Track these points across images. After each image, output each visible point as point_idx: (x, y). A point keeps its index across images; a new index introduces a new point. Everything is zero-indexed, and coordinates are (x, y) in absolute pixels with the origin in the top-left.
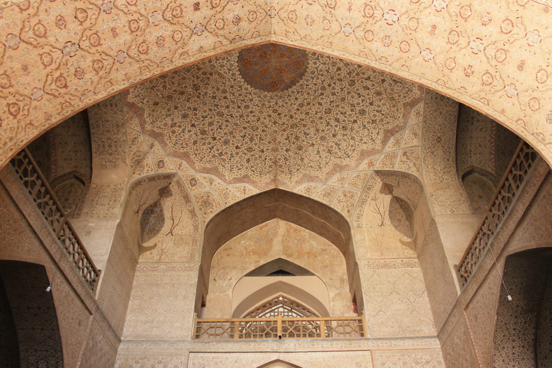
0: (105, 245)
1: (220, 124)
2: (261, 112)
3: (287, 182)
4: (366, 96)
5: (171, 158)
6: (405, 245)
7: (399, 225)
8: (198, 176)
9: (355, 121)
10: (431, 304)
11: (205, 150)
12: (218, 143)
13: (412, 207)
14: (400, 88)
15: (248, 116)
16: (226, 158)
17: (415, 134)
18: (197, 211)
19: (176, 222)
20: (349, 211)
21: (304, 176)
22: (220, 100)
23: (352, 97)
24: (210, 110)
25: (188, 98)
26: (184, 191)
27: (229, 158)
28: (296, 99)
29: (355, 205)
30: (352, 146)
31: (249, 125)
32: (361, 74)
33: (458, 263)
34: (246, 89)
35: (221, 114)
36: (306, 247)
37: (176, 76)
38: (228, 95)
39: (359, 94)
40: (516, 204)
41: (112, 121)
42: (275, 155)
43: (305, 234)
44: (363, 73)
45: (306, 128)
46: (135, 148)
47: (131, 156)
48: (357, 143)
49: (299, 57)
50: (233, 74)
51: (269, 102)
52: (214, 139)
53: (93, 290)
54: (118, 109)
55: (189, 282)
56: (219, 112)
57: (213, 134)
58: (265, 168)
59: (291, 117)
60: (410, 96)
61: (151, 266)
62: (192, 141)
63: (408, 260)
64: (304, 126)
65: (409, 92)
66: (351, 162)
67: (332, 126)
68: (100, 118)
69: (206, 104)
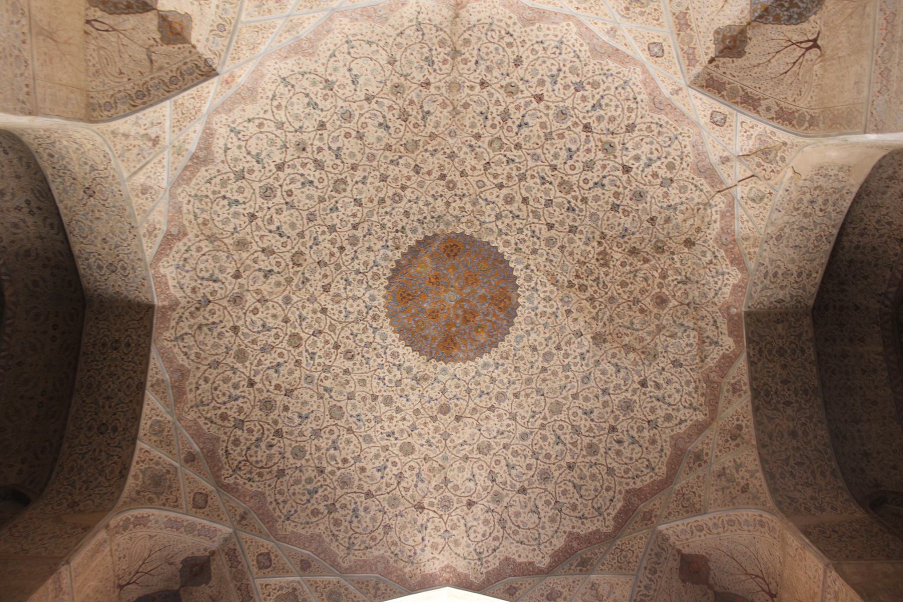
1: (570, 162)
2: (481, 184)
4: (267, 233)
5: (693, 117)
8: (643, 56)
9: (280, 168)
11: (613, 104)
12: (581, 116)
14: (202, 266)
15: (509, 177)
17: (145, 190)
21: (387, 19)
22: (562, 223)
23: (293, 226)
24: (584, 200)
25: (624, 236)
26: (682, 42)
27: (562, 75)
30: (279, 107)
32: (283, 282)
37: (636, 293)
38: (545, 233)
39: (281, 235)
41: (787, 246)
42: (455, 74)
44: (278, 284)
45: (385, 141)
46: (762, 186)
48: (269, 116)
49: (403, 311)
50: (529, 279)
52: (587, 128)
56: (568, 193)
57: (587, 141)
58: (479, 39)
59: (417, 170)
60: (177, 256)
64: (389, 147)
65: (181, 263)
66: (274, 68)
67: (330, 148)
68: (808, 252)
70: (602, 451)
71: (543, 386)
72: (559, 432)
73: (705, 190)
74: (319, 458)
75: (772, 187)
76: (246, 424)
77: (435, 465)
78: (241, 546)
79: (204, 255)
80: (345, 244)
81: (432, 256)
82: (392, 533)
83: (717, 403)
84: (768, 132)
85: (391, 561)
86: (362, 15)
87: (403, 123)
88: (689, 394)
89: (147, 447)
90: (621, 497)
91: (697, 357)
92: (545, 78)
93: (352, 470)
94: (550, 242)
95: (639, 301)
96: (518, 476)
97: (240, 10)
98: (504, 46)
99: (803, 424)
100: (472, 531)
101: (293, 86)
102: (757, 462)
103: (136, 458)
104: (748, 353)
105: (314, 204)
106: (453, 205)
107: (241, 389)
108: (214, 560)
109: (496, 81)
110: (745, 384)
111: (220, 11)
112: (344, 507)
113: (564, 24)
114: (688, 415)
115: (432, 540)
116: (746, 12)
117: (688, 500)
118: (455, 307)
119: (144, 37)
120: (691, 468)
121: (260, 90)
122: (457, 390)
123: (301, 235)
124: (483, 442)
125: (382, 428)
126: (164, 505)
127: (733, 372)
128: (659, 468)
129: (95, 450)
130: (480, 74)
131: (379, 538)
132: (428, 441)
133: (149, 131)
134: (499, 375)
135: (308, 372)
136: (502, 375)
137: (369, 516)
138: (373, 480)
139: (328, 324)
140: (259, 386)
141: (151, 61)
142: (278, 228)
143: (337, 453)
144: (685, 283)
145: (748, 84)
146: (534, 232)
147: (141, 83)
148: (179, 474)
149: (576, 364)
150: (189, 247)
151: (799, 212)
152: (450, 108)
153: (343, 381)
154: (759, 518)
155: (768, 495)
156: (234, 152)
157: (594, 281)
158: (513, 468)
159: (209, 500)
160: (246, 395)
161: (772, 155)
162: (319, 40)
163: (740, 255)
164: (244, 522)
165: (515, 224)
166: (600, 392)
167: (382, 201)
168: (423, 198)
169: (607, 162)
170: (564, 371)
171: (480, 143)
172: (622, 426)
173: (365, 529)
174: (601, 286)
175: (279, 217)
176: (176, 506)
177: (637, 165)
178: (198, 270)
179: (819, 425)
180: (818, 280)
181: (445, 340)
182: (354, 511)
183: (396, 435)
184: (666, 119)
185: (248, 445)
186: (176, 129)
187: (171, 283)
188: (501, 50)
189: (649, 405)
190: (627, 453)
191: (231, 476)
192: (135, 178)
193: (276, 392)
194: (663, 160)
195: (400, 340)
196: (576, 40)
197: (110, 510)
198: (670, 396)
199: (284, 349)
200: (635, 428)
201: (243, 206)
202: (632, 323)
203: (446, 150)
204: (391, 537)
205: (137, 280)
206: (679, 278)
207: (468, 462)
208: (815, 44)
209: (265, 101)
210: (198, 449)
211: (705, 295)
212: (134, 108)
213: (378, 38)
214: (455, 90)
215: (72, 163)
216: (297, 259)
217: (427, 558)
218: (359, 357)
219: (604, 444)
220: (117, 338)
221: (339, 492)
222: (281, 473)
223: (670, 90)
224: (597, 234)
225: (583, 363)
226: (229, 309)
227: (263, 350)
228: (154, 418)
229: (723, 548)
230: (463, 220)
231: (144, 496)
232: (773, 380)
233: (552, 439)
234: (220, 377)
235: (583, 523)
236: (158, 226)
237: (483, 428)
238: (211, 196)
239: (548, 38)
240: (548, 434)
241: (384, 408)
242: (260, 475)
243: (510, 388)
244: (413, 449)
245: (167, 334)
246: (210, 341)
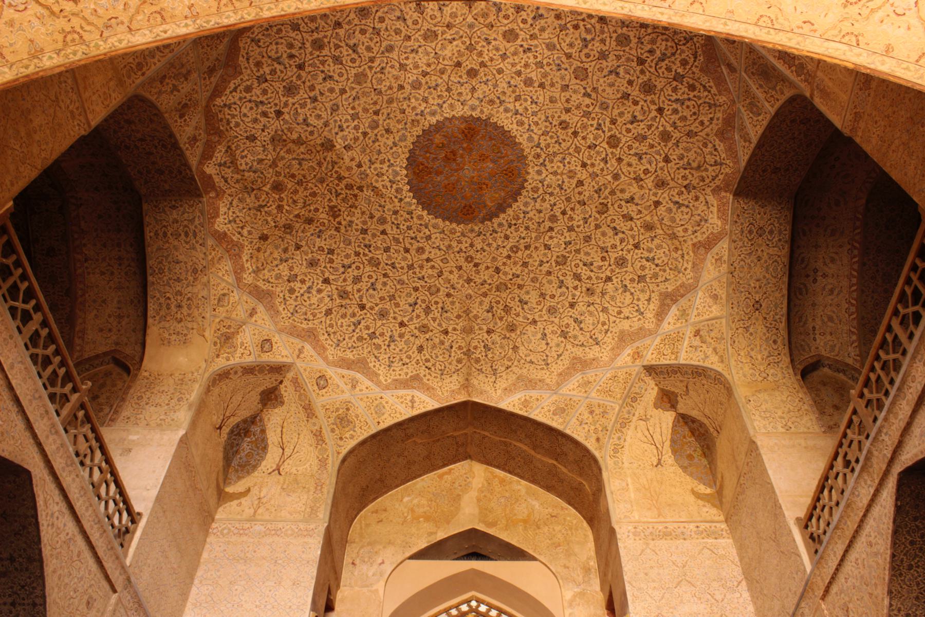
0: (154, 472)
1: (373, 280)
3: (488, 389)
4: (627, 232)
5: (284, 336)
6: (702, 499)
7: (690, 465)
8: (331, 372)
10: (755, 603)
11: (345, 328)
12: (368, 315)
13: (712, 430)
14: (686, 217)
15: (421, 267)
17: (715, 297)
18: (326, 433)
19: (288, 452)
20: (598, 440)
21: (518, 378)
22: (374, 236)
24: (357, 254)
25: (320, 231)
26: (306, 396)
27: (387, 343)
28: (507, 237)
29: (609, 429)
30: (604, 324)
31: (424, 284)
33: (802, 513)
34: (420, 217)
36: (521, 511)
37: (301, 189)
38: (388, 227)
39: (615, 228)
40: (910, 366)
41: (186, 263)
43: (519, 487)
44: (622, 191)
48: (612, 319)
49: (512, 161)
51: (460, 242)
52: (363, 307)
53: (122, 545)
54: (197, 242)
55: (304, 556)
56: (372, 258)
57: (361, 298)
59: (497, 270)
60: (704, 230)
61: (237, 525)
62: (324, 310)
63: (708, 525)
64: (520, 287)
65: (703, 223)
66: (602, 353)
67: (567, 288)
68: (167, 257)
69: (350, 244)
70: (308, 45)
72: (354, 56)
81: (485, 206)
88: (233, 116)
89: (767, 104)
92: (398, 339)
95: (298, 183)
97: (618, 414)
99: (123, 128)
101: (591, 337)
103: (778, 105)
104: (191, 170)
106: (467, 245)
107: (671, 108)
110: (187, 149)
113: (389, 381)
114: (230, 97)
116: (266, 419)
118: (464, 164)
120: (217, 59)
123: (597, 227)
124: (432, 42)
125: (535, 57)
127: (199, 151)
132: (489, 43)
134: (420, 105)
136: (417, 106)
140: (653, 107)
143: (584, 35)
144: (261, 206)
149: (347, 121)
152: (471, 315)
154: (144, 69)
156: (643, 297)
158: (399, 18)
160: (666, 102)
162: (568, 368)
163: (220, 243)
166: (319, 98)
167: (527, 247)
168: (493, 249)
172: (292, 72)
180: (147, 230)
183: (521, 49)
184: (303, 326)
185: (673, 59)
186: (681, 334)
187: (715, 210)
188: (434, 356)
189: (269, 95)
190: (282, 48)
195: (515, 137)
198: (251, 108)
200: (279, 73)
202: (300, 164)
205: (742, 221)
207: (446, 22)
210: (723, 67)
211: (240, 200)
214: (468, 328)
216: (603, 209)
218: (554, 123)
223: (305, 350)
224: (343, 230)
227: (645, 138)
228: (755, 119)
230: (459, 234)
233: (361, 49)
234: (688, 123)
236: (714, 261)
237: (433, 55)
240: (366, 53)
241: (533, 75)
244: (504, 36)
245: (727, 170)
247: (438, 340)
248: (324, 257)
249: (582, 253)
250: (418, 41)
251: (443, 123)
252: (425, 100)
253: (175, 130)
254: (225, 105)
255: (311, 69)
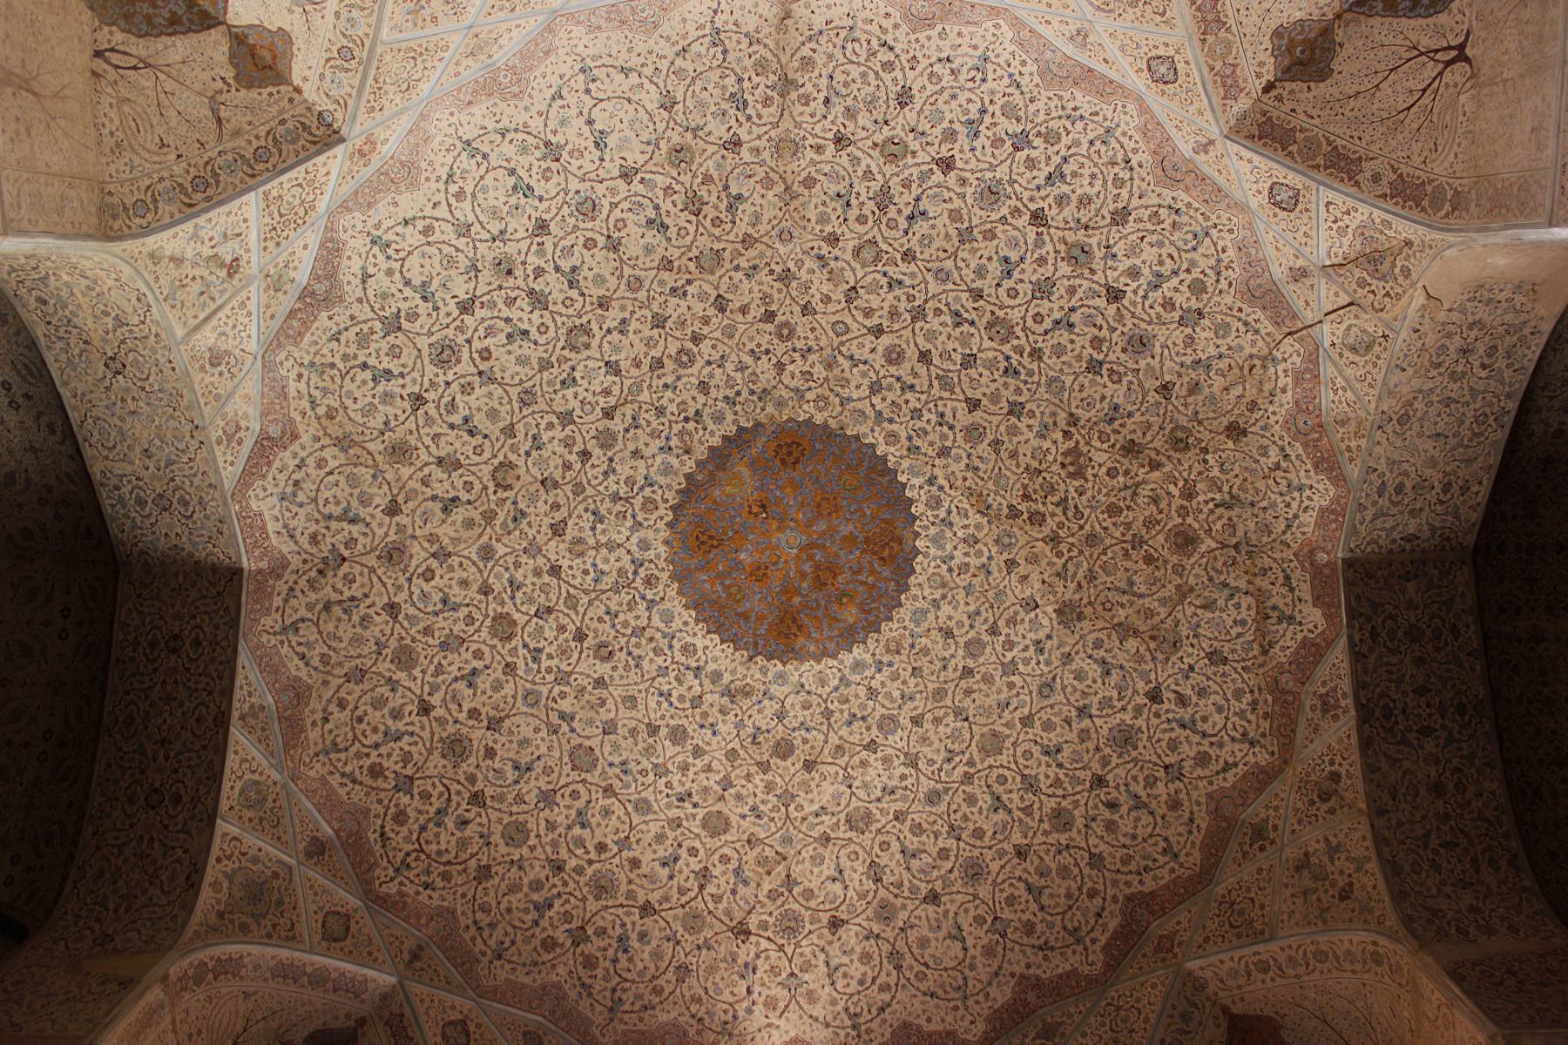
1: (1007, 284)
4: (445, 430)
5: (1238, 195)
8: (1139, 82)
9: (466, 308)
11: (1086, 172)
12: (1026, 195)
14: (328, 494)
15: (894, 314)
16: (1000, 119)
21: (656, 26)
22: (995, 398)
23: (493, 414)
24: (1036, 354)
25: (1112, 420)
26: (1211, 54)
27: (988, 120)
28: (704, 387)
31: (890, 270)
35: (999, 328)
38: (964, 418)
39: (471, 433)
41: (1420, 435)
42: (787, 123)
44: (469, 524)
45: (660, 251)
46: (1370, 324)
47: (1396, 311)
48: (442, 212)
51: (807, 375)
52: (1038, 218)
56: (1005, 341)
57: (1039, 243)
58: (830, 57)
59: (721, 304)
60: (282, 477)
65: (289, 489)
67: (557, 269)
68: (1460, 444)
70: (1080, 822)
71: (967, 702)
73: (1263, 332)
74: (554, 844)
75: (1387, 325)
76: (417, 783)
77: (768, 852)
78: (412, 1010)
79: (331, 473)
80: (591, 445)
81: (753, 464)
82: (692, 981)
83: (1293, 731)
84: (1378, 221)
85: (692, 1032)
86: (609, 20)
87: (693, 218)
88: (1241, 714)
90: (1116, 908)
91: (1255, 646)
92: (957, 127)
93: (615, 864)
94: (974, 433)
95: (1142, 542)
96: (923, 871)
97: (380, 20)
98: (878, 68)
99: (1457, 770)
100: (839, 974)
101: (485, 156)
102: (1368, 843)
103: (215, 851)
104: (1350, 638)
105: (531, 373)
106: (790, 368)
107: (407, 719)
108: (364, 1035)
109: (864, 134)
110: (1345, 696)
111: (342, 24)
112: (601, 932)
113: (990, 24)
114: (1239, 755)
115: (765, 992)
117: (1241, 914)
118: (797, 557)
119: (206, 76)
120: (1245, 854)
121: (424, 165)
122: (806, 713)
123: (510, 431)
124: (856, 809)
125: (668, 785)
126: (269, 936)
127: (1322, 672)
128: (1187, 855)
129: (141, 838)
130: (833, 123)
131: (668, 988)
132: (753, 809)
133: (220, 250)
134: (883, 684)
135: (528, 685)
136: (888, 683)
137: (648, 949)
138: (653, 882)
139: (564, 594)
141: (219, 120)
142: (466, 420)
143: (586, 833)
144: (1229, 507)
145: (1340, 132)
146: (942, 415)
147: (201, 163)
148: (297, 879)
149: (1026, 662)
150: (303, 460)
151: (1442, 370)
152: (780, 188)
153: (593, 699)
154: (1371, 948)
155: (1388, 904)
156: (380, 282)
157: (1058, 505)
159: (352, 925)
160: (417, 730)
161: (1387, 265)
164: (418, 965)
165: (907, 402)
166: (1074, 713)
167: (658, 364)
168: (733, 357)
169: (1078, 281)
170: (1004, 674)
171: (836, 252)
172: (1115, 776)
173: (641, 974)
174: (1070, 514)
175: (467, 398)
176: (291, 937)
177: (1135, 285)
178: (321, 502)
179: (1488, 770)
180: (1483, 498)
181: (782, 621)
182: (620, 939)
183: (695, 799)
184: (1187, 199)
186: (270, 244)
188: (872, 75)
189: (1167, 736)
190: (1126, 825)
191: (392, 880)
192: (198, 336)
193: (471, 723)
194: (1183, 276)
195: (697, 621)
196: (1013, 54)
197: (170, 948)
198: (1205, 719)
199: (484, 642)
200: (1140, 779)
201: (401, 381)
202: (1132, 584)
203: (773, 266)
204: (690, 988)
205: (209, 523)
206: (1218, 496)
208: (1462, 57)
209: (433, 185)
210: (331, 832)
212: (190, 210)
213: (641, 60)
215: (81, 315)
216: (503, 475)
217: (757, 1026)
219: (1083, 809)
220: (176, 631)
221: (592, 905)
222: (485, 872)
223: (1192, 144)
224: (1062, 417)
225: (1041, 658)
226: (380, 572)
227: (444, 646)
228: (248, 776)
229: (1306, 1004)
230: (810, 396)
231: (232, 922)
232: (1397, 688)
233: (985, 801)
235: (1046, 958)
236: (243, 424)
238: (341, 366)
239: (959, 51)
240: (978, 792)
241: (671, 750)
242: (446, 876)
243: (905, 708)
244: (727, 823)
245: (267, 622)
246: (346, 631)
247: (861, 122)
248: (1112, 357)
249: (535, 361)
250: (881, 810)
251: (839, 648)
252: (872, 693)
253: (1355, 757)
254: (1252, 744)
255: (1081, 774)
